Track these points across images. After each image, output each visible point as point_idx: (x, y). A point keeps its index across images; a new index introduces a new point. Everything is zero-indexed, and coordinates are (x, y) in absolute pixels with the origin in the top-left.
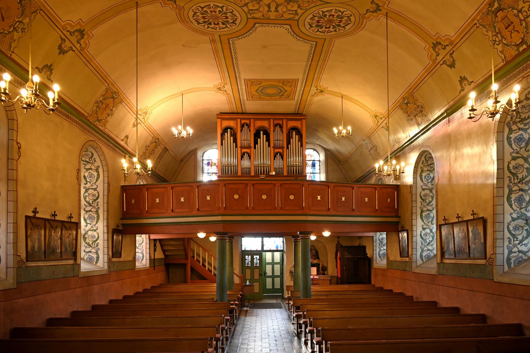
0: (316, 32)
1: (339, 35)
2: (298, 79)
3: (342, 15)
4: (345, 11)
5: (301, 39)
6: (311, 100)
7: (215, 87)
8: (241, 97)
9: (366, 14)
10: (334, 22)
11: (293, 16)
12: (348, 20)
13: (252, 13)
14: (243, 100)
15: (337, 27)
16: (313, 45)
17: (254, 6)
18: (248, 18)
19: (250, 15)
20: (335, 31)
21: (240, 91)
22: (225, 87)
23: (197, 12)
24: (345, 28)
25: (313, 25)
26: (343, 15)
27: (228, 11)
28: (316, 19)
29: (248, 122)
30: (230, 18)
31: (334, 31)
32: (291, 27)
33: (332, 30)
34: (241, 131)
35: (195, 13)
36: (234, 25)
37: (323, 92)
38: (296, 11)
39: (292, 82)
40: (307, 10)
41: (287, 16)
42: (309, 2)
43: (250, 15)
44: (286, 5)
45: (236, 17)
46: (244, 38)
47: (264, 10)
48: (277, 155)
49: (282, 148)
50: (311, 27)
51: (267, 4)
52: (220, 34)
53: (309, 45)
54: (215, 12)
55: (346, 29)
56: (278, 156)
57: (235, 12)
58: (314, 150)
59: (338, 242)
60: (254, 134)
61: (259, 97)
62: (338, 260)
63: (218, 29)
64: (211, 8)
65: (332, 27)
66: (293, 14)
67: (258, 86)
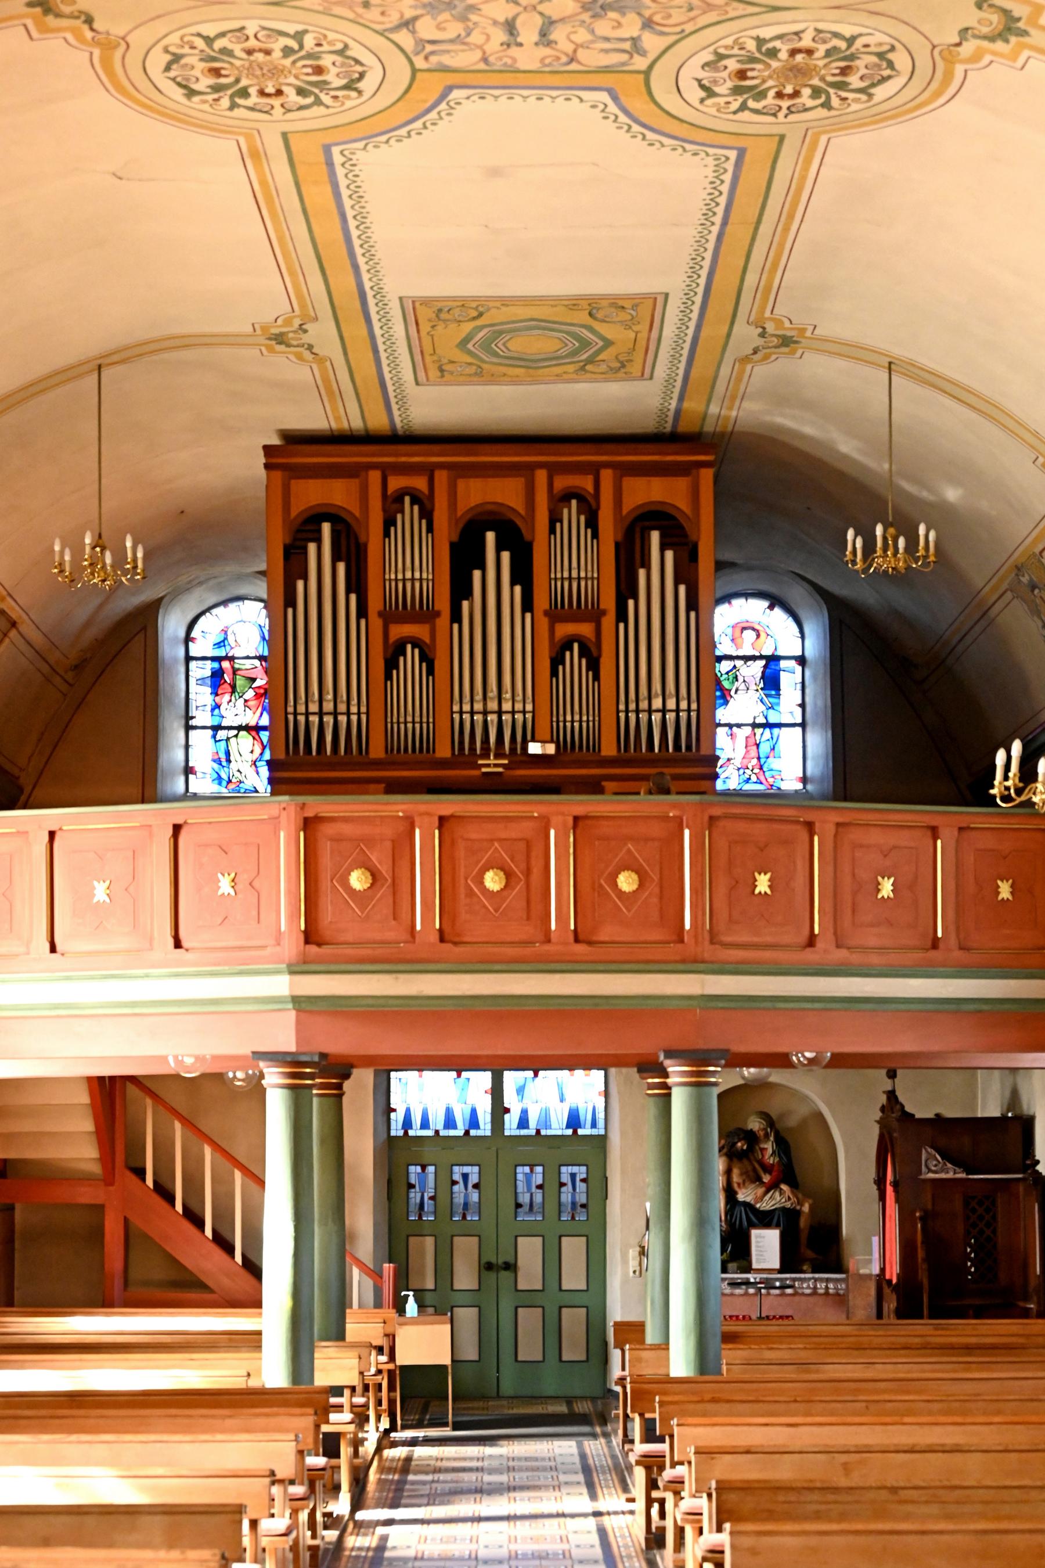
0: (735, 113)
1: (844, 118)
2: (667, 295)
3: (849, 47)
4: (861, 35)
5: (666, 141)
6: (739, 380)
7: (258, 332)
8: (386, 370)
9: (959, 44)
10: (818, 74)
11: (625, 57)
12: (879, 66)
13: (433, 53)
14: (399, 383)
15: (832, 91)
16: (727, 159)
17: (444, 29)
18: (414, 71)
19: (426, 58)
20: (827, 105)
21: (381, 348)
22: (305, 331)
23: (182, 56)
24: (870, 96)
25: (717, 89)
26: (853, 49)
27: (326, 47)
28: (733, 65)
29: (420, 483)
30: (334, 71)
31: (822, 105)
32: (615, 99)
33: (810, 103)
34: (387, 534)
35: (177, 58)
36: (354, 94)
37: (796, 342)
38: (635, 41)
39: (637, 305)
40: (683, 36)
41: (591, 58)
42: (691, 9)
43: (426, 58)
44: (588, 20)
45: (359, 68)
46: (398, 141)
47: (488, 38)
48: (568, 654)
49: (595, 616)
50: (710, 93)
51: (501, 19)
52: (287, 127)
53: (704, 162)
54: (268, 52)
55: (876, 99)
56: (574, 656)
57: (356, 51)
58: (775, 601)
59: (891, 1095)
60: (452, 545)
61: (473, 369)
62: (889, 1190)
63: (278, 111)
64: (248, 38)
65: (806, 92)
66: (624, 51)
67: (467, 327)
